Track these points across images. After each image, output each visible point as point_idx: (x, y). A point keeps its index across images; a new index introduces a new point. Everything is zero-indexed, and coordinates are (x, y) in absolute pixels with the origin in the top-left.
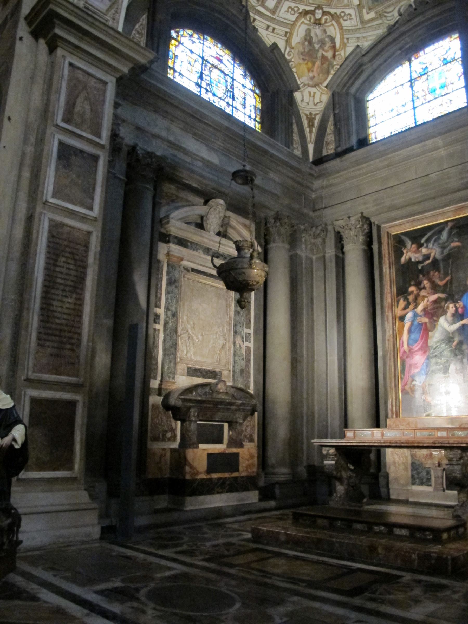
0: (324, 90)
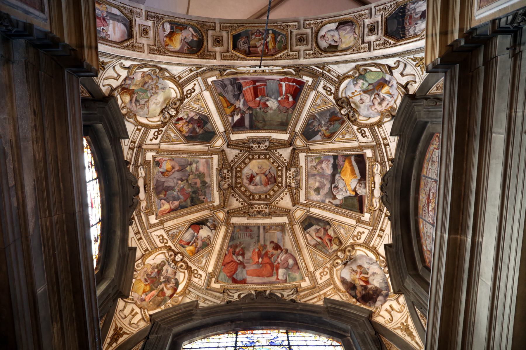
0: (146, 317)
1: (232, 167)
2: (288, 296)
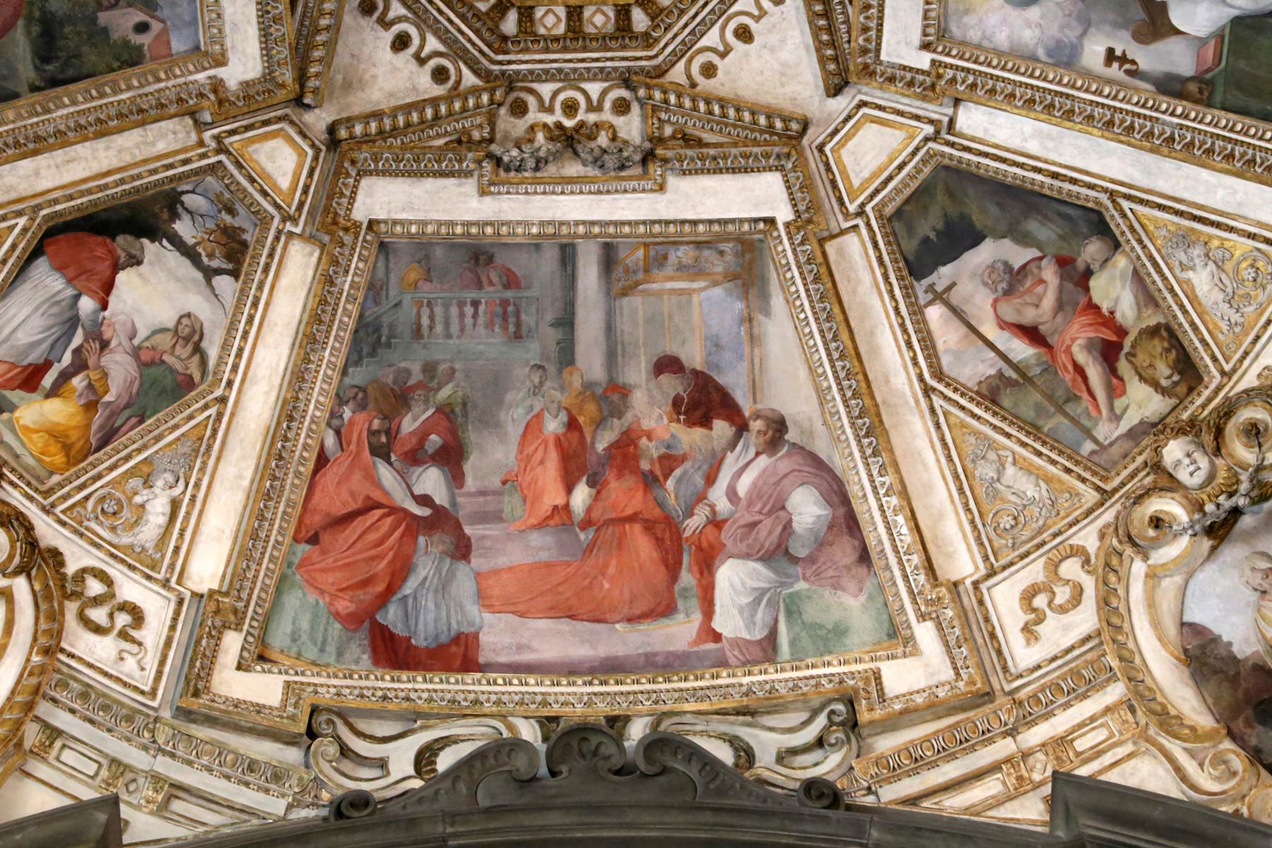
2: (786, 756)
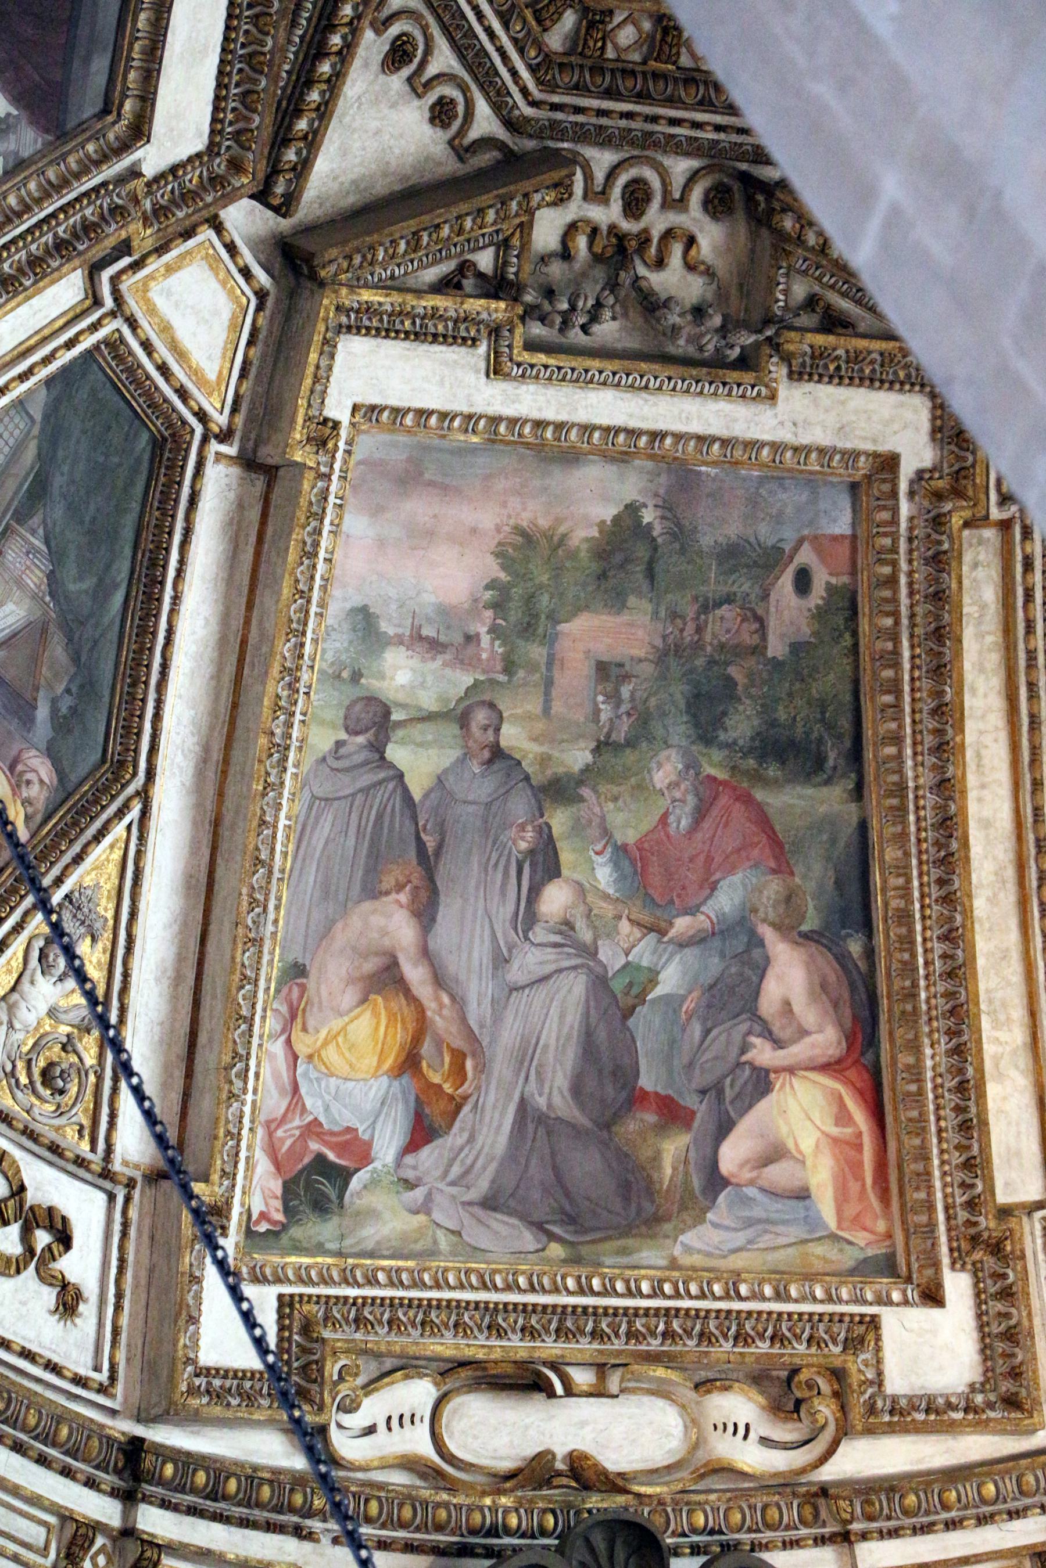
1: (510, 124)
